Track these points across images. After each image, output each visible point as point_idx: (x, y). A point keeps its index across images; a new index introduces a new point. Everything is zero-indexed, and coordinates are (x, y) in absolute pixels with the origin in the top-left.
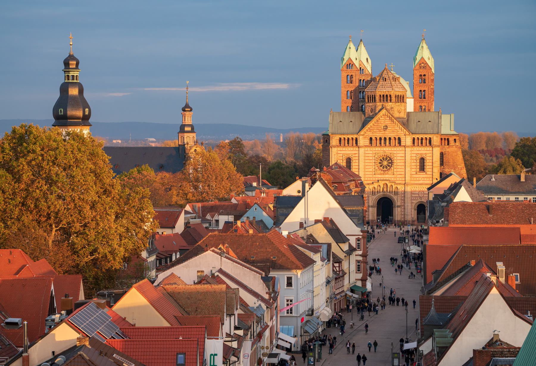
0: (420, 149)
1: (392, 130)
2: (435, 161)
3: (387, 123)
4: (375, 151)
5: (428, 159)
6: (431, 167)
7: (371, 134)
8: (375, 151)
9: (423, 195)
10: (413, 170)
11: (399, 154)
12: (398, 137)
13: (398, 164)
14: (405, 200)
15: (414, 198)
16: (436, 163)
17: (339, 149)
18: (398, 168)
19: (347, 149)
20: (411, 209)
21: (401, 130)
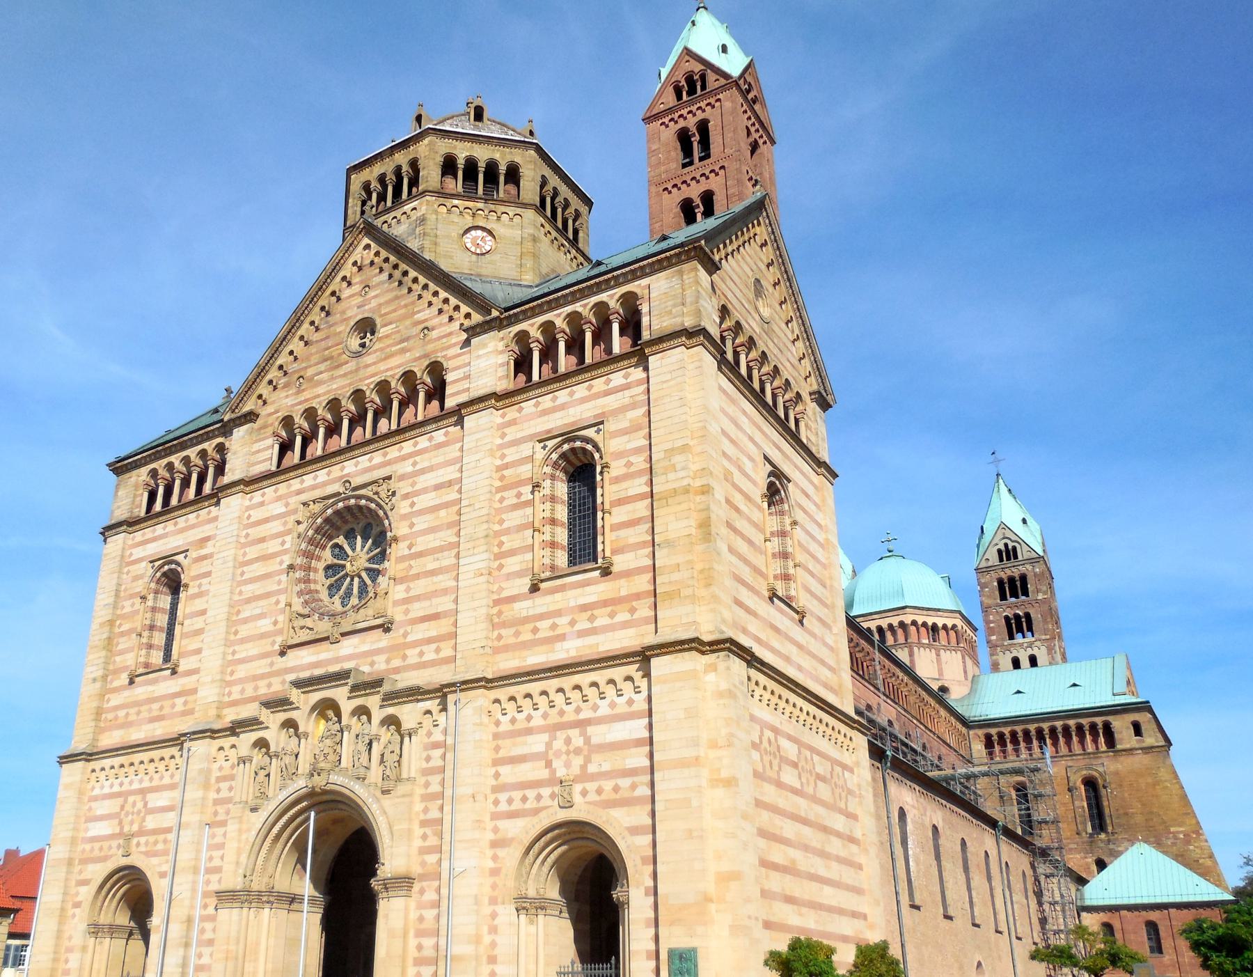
0: (563, 396)
1: (397, 337)
2: (670, 452)
3: (374, 303)
4: (299, 492)
5: (620, 455)
6: (642, 508)
7: (290, 401)
8: (299, 492)
9: (578, 761)
10: (513, 564)
11: (431, 469)
12: (427, 363)
13: (422, 543)
14: (440, 821)
15: (517, 795)
16: (678, 459)
17: (138, 536)
18: (417, 576)
19: (170, 526)
20: (493, 901)
21: (445, 318)
